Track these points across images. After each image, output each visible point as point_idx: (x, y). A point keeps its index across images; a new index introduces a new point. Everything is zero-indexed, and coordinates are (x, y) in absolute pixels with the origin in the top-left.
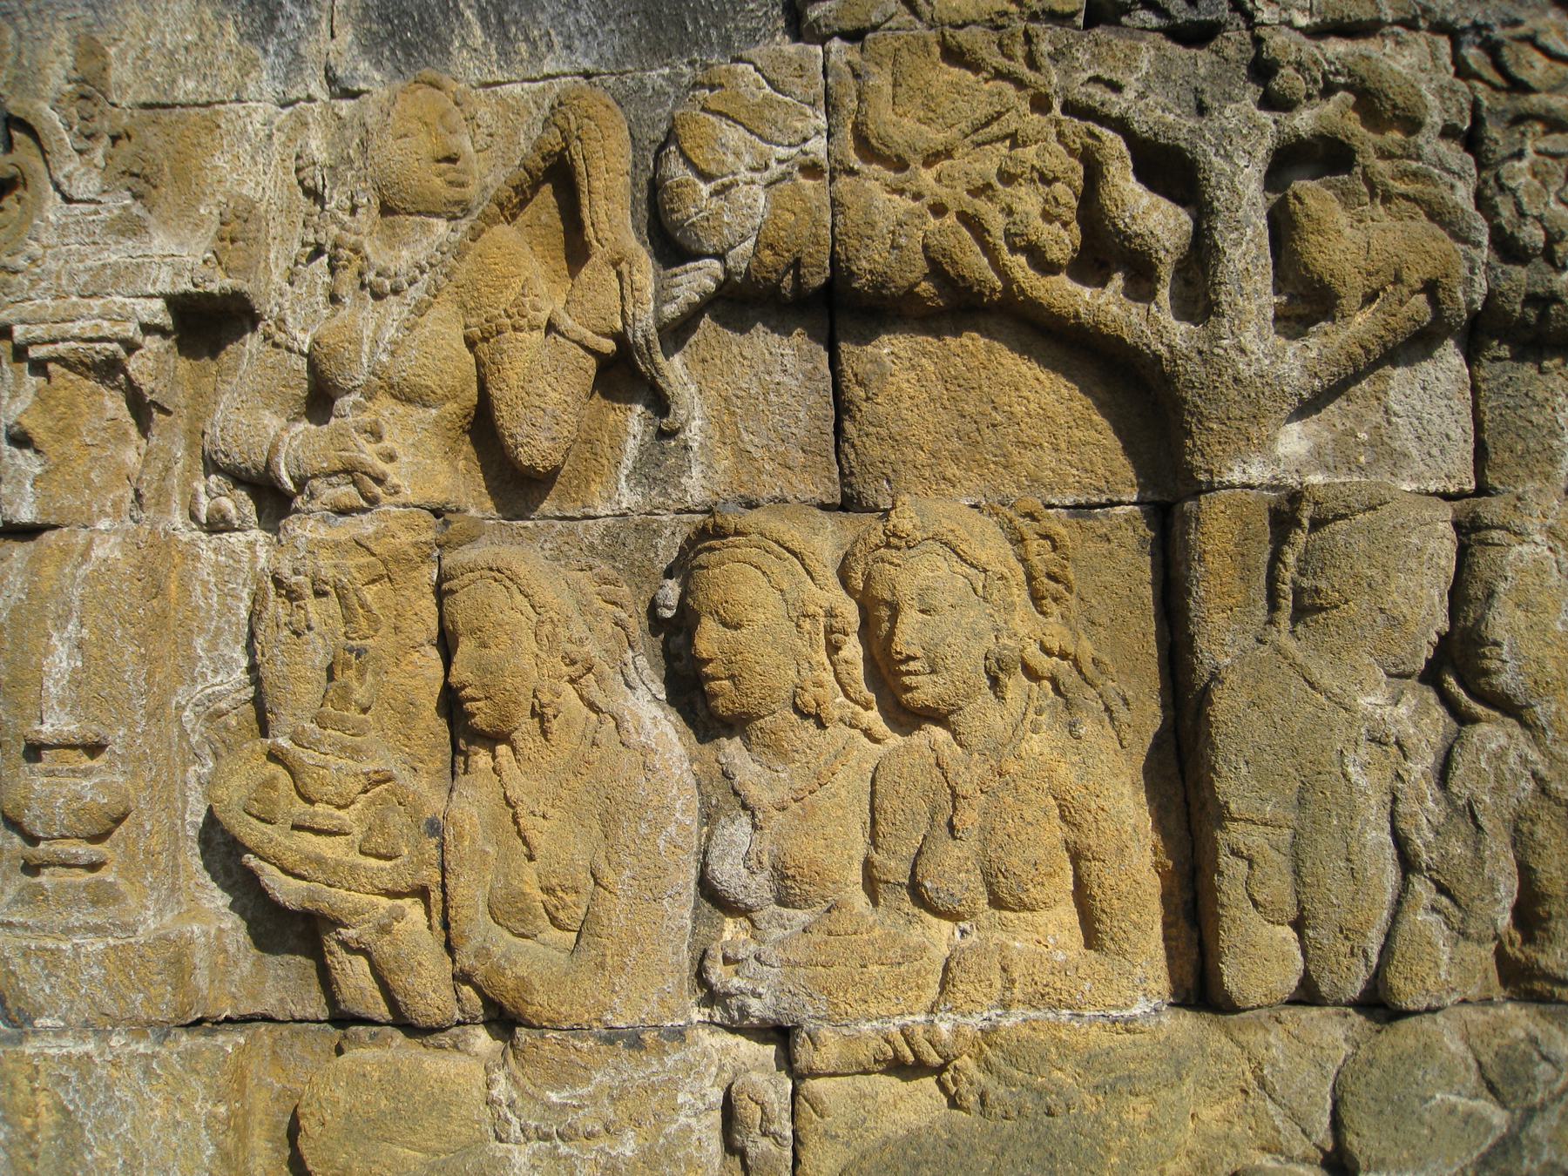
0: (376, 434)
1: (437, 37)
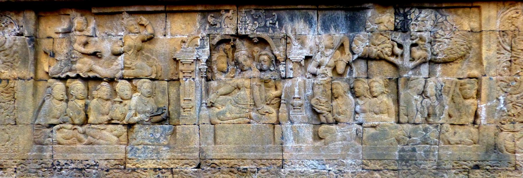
0: (326, 70)
1: (329, 29)
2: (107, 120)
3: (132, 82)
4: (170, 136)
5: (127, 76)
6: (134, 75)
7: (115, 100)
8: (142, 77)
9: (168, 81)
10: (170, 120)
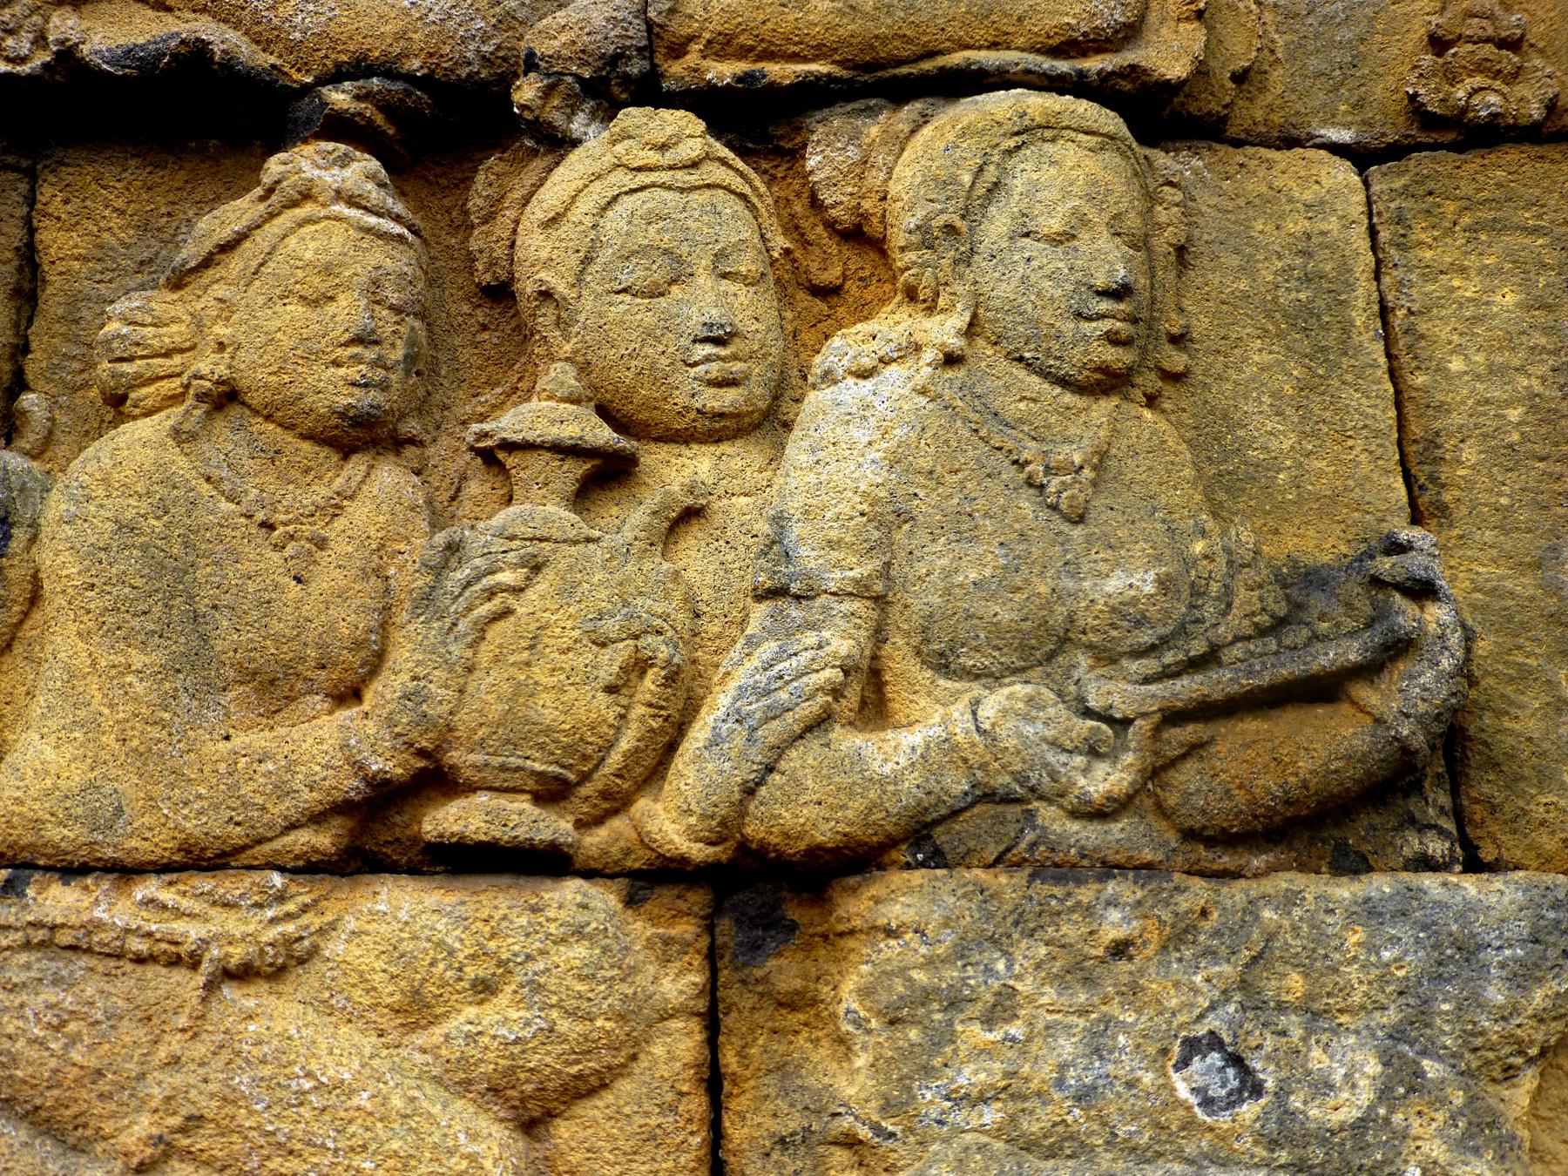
2: (351, 785)
3: (796, 155)
4: (1528, 1081)
5: (723, 47)
6: (849, 27)
7: (511, 423)
8: (989, 58)
9: (1360, 157)
10: (1485, 786)
